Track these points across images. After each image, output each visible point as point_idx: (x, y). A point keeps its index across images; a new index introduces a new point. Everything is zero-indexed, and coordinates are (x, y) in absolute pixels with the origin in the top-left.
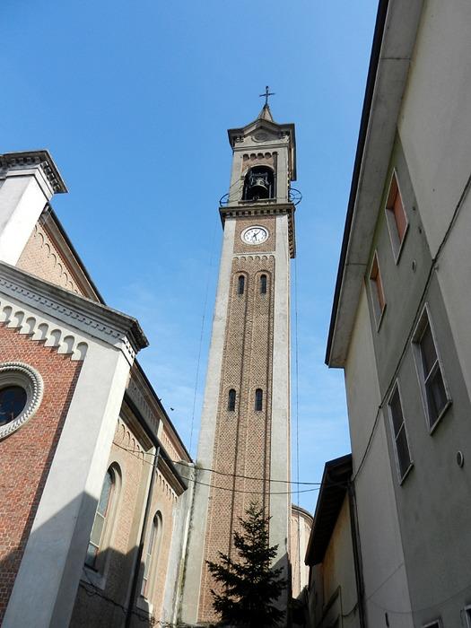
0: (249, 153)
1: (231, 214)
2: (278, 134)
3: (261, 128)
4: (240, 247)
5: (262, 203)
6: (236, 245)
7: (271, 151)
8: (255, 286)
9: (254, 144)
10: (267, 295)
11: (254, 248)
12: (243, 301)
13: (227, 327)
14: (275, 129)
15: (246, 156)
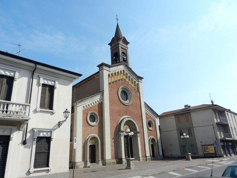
7: (126, 48)
9: (122, 44)
15: (121, 47)
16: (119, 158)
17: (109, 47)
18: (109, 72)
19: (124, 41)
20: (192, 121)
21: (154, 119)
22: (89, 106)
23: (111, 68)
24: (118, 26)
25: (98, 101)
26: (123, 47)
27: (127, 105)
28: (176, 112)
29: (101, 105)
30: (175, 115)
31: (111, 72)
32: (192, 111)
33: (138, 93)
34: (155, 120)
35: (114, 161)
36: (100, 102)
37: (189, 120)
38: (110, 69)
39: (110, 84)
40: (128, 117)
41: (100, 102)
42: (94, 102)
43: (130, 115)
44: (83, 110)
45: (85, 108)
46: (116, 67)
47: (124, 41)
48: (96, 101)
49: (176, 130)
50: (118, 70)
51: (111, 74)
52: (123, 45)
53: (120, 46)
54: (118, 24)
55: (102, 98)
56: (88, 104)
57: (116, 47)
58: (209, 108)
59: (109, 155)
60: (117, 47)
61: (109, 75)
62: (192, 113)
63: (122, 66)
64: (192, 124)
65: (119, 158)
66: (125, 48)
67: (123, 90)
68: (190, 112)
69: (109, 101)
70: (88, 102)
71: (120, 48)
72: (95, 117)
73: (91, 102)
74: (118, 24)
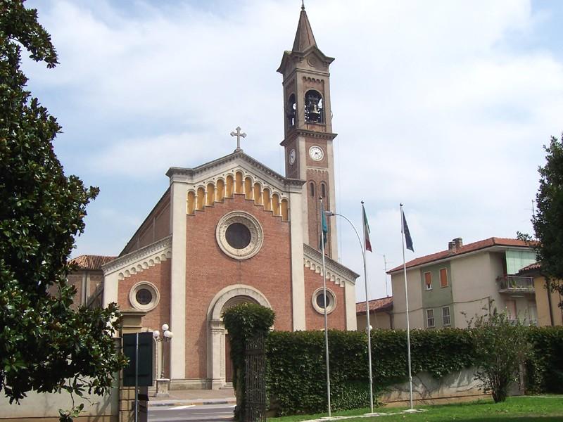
0: (307, 76)
1: (303, 134)
2: (323, 62)
3: (313, 52)
4: (310, 162)
5: (317, 129)
6: (307, 159)
7: (320, 78)
8: (319, 192)
9: (308, 68)
10: (326, 198)
11: (317, 163)
12: (314, 201)
13: (309, 217)
14: (321, 57)
15: (304, 78)
16: (208, 377)
17: (280, 77)
18: (191, 187)
19: (315, 54)
20: (451, 286)
21: (342, 286)
22: (135, 271)
23: (197, 179)
24: (303, 14)
25: (157, 258)
26: (312, 76)
27: (241, 258)
28: (425, 261)
29: (167, 266)
30: (421, 269)
31: (196, 185)
32: (455, 260)
33: (288, 224)
34: (344, 288)
35: (198, 383)
36: (165, 260)
37: (445, 282)
38: (194, 177)
39: (191, 215)
40: (238, 289)
41: (165, 260)
42: (147, 260)
43: (251, 282)
44: (120, 281)
45: (126, 275)
46: (215, 168)
47: (315, 54)
48: (154, 259)
49: (422, 310)
50: (221, 175)
51: (196, 189)
52: (310, 72)
53: (299, 76)
54: (303, 8)
55: (168, 250)
56: (132, 266)
57: (291, 79)
58: (485, 252)
59: (178, 370)
60: (294, 80)
61: (191, 193)
62: (452, 266)
63: (233, 161)
64: (452, 295)
65: (208, 377)
66: (316, 77)
67: (236, 222)
68: (449, 262)
69: (188, 254)
70: (131, 262)
71: (300, 81)
72: (152, 292)
73: (138, 263)
74: (303, 8)
